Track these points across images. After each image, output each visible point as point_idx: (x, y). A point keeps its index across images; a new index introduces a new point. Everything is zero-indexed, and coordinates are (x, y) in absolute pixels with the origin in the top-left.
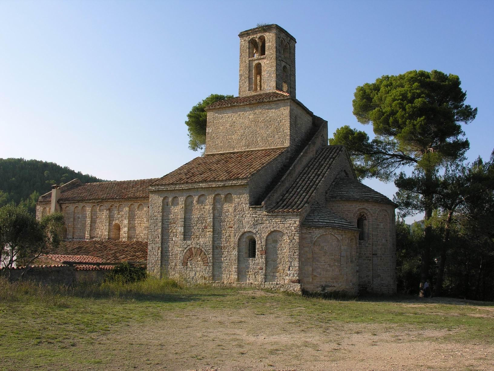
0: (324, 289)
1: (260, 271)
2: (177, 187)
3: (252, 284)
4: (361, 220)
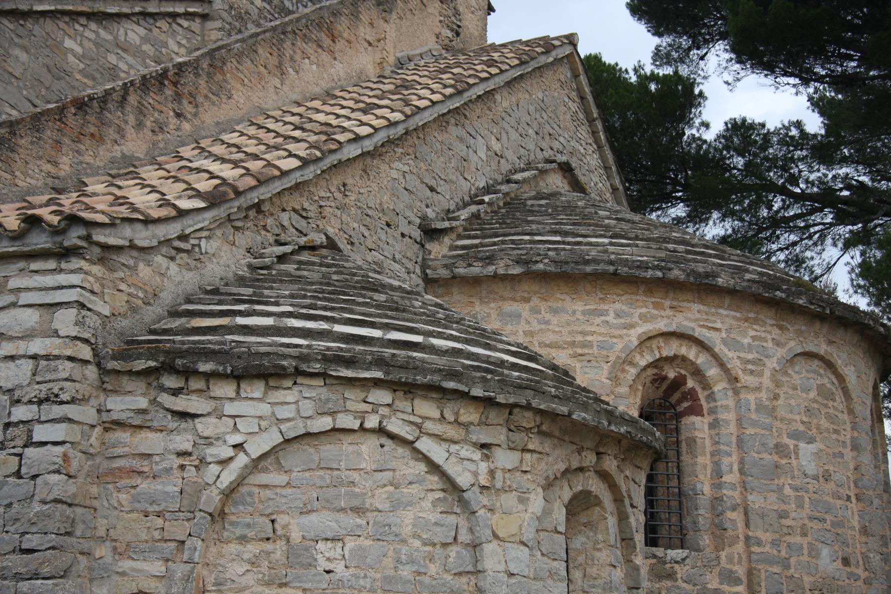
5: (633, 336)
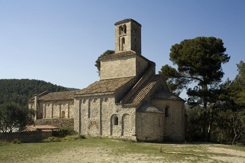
0: (146, 138)
1: (120, 131)
2: (85, 95)
4: (167, 109)
5: (165, 103)
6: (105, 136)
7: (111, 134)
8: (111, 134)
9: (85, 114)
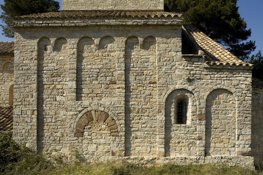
1: (198, 142)
3: (186, 158)
6: (142, 159)
7: (167, 152)
8: (167, 152)
9: (59, 87)
